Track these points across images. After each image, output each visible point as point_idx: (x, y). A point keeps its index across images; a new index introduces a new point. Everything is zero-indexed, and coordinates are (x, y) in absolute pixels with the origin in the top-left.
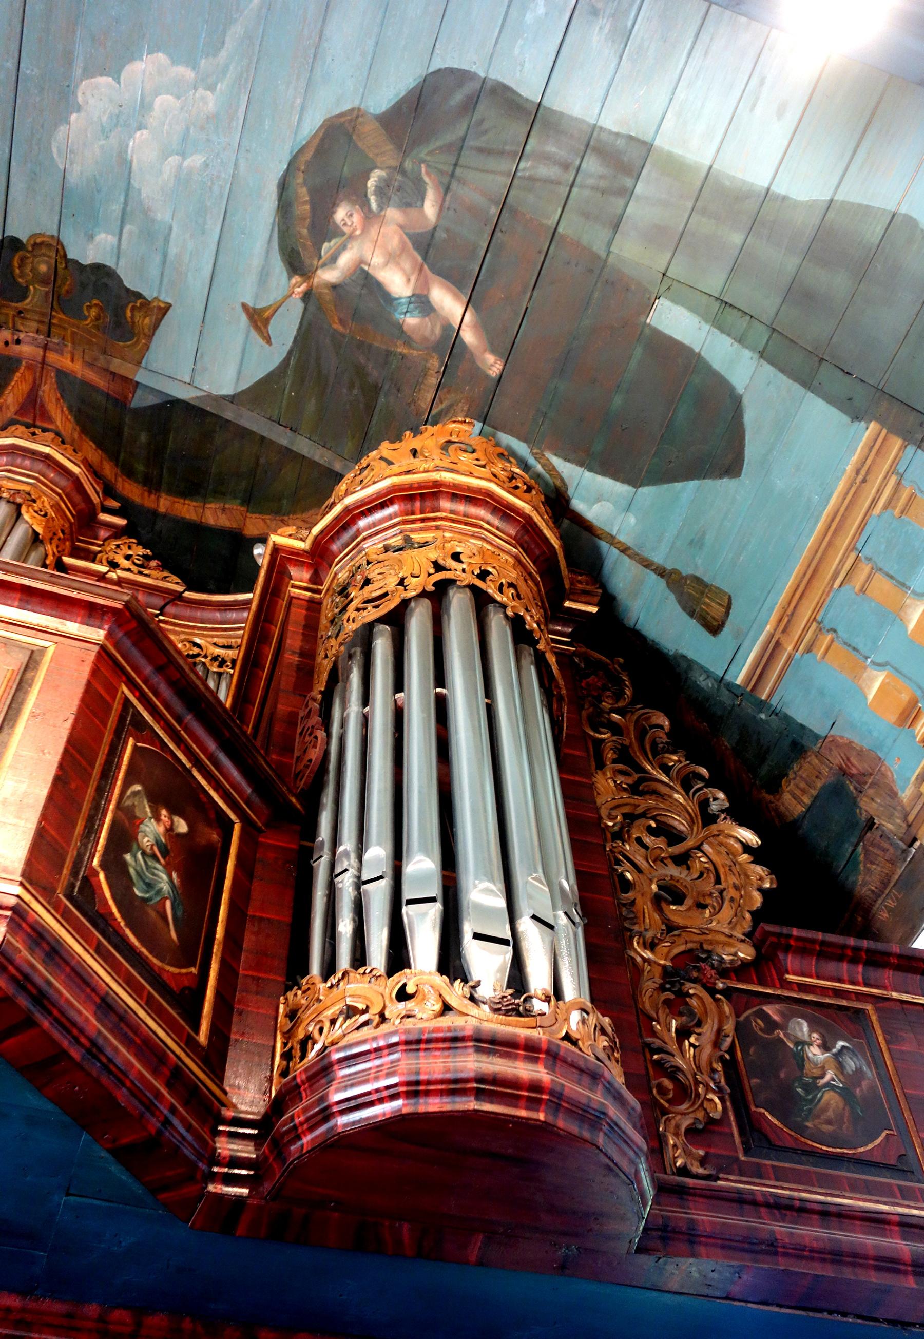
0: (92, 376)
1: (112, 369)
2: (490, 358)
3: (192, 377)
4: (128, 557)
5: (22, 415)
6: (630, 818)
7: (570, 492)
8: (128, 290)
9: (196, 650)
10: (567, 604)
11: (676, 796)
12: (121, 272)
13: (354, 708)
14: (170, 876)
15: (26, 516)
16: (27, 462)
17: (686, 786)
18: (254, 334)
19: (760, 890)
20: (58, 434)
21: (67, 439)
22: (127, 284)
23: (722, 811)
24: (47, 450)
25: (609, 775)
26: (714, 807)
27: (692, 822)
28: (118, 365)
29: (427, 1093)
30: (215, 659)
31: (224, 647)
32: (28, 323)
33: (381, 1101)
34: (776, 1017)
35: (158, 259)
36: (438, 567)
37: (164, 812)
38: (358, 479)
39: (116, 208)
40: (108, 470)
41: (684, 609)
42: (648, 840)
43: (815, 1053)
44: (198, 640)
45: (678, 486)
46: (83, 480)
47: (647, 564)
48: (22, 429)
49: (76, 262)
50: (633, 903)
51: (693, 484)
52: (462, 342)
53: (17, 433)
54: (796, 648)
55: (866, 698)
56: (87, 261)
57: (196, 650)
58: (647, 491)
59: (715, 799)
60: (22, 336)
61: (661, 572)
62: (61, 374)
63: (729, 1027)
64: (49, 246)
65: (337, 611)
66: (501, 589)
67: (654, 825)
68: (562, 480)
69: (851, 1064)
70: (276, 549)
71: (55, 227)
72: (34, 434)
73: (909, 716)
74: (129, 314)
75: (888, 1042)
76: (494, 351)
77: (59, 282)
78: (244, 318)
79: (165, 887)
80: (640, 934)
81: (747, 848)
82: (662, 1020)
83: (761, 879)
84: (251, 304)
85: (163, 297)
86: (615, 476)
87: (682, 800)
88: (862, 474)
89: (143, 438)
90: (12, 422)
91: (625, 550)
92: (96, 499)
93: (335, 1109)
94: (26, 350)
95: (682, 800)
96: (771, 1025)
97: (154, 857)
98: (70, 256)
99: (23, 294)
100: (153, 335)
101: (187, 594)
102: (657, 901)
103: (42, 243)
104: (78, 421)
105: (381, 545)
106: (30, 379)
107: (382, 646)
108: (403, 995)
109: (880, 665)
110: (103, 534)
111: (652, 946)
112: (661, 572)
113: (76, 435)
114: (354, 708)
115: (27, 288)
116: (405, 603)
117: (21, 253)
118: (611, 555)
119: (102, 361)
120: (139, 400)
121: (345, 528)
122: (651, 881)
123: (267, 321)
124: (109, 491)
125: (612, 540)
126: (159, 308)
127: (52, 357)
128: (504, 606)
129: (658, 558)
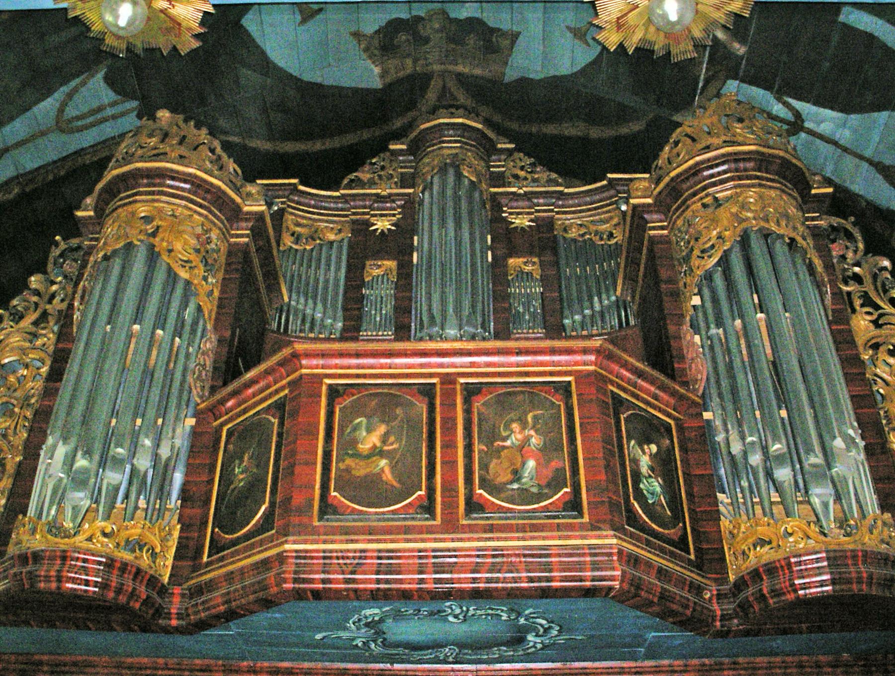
2: (736, 45)
4: (522, 168)
6: (876, 347)
14: (658, 481)
18: (578, 42)
24: (460, 120)
29: (810, 588)
37: (646, 447)
38: (675, 151)
40: (497, 118)
47: (861, 157)
58: (855, 118)
66: (778, 223)
67: (891, 347)
70: (635, 207)
78: (569, 35)
84: (573, 26)
85: (515, 28)
86: (832, 109)
97: (650, 476)
101: (566, 191)
107: (719, 281)
112: (870, 162)
120: (507, 79)
123: (585, 34)
128: (781, 237)
129: (868, 153)
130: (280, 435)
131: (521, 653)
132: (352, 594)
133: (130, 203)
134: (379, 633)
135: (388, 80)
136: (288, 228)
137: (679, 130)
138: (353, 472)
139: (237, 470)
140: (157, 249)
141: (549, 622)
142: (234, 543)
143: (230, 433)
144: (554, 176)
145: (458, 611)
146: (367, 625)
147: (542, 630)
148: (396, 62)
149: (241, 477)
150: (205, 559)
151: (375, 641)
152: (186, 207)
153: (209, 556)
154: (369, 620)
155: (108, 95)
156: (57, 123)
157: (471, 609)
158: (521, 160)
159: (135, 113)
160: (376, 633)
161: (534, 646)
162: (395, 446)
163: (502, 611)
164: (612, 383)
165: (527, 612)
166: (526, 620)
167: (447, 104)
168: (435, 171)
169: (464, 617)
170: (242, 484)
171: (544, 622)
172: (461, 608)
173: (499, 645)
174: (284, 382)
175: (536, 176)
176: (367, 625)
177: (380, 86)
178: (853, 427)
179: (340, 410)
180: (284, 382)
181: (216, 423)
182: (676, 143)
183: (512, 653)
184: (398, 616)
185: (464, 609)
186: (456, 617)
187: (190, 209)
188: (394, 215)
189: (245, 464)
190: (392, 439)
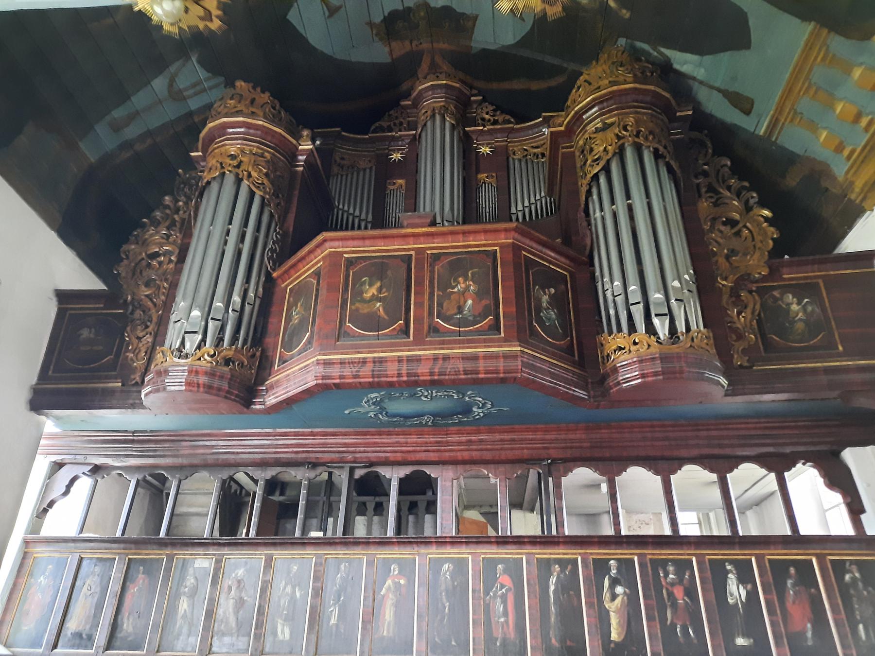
2: (624, 11)
3: (495, 40)
4: (487, 113)
6: (714, 220)
7: (672, 61)
9: (526, 153)
10: (678, 114)
11: (734, 202)
12: (454, 6)
13: (598, 214)
14: (554, 312)
15: (448, 119)
17: (738, 195)
19: (773, 239)
22: (458, 10)
23: (755, 203)
25: (704, 200)
26: (752, 201)
27: (741, 215)
29: (648, 377)
30: (534, 154)
31: (537, 147)
33: (634, 380)
34: (778, 296)
36: (619, 138)
38: (578, 93)
41: (732, 105)
42: (722, 228)
43: (795, 307)
44: (525, 148)
45: (722, 54)
47: (712, 87)
49: (435, 8)
50: (717, 261)
51: (728, 53)
52: (610, 6)
54: (786, 120)
55: (819, 140)
56: (439, 6)
57: (526, 153)
58: (708, 59)
59: (752, 197)
60: (422, 41)
61: (719, 90)
63: (758, 307)
65: (582, 163)
68: (667, 57)
69: (810, 308)
72: (438, 77)
73: (839, 149)
74: (461, 21)
75: (827, 294)
76: (626, 8)
79: (554, 316)
80: (721, 275)
81: (766, 219)
82: (731, 310)
83: (773, 233)
85: (474, 12)
86: (692, 53)
87: (736, 204)
88: (809, 47)
90: (428, 74)
91: (701, 82)
92: (468, 93)
93: (622, 382)
95: (736, 204)
96: (776, 299)
100: (474, 26)
102: (728, 257)
105: (594, 128)
107: (602, 180)
108: (635, 343)
109: (825, 128)
110: (475, 106)
111: (726, 279)
112: (719, 90)
114: (598, 214)
115: (418, 23)
116: (608, 162)
118: (696, 86)
120: (473, 52)
121: (578, 119)
122: (724, 249)
124: (471, 88)
125: (694, 79)
126: (473, 17)
127: (435, 45)
129: (717, 85)
130: (317, 290)
131: (472, 419)
132: (358, 385)
133: (223, 146)
134: (382, 409)
136: (336, 161)
137: (581, 78)
140: (240, 177)
141: (483, 399)
142: (292, 357)
144: (508, 117)
145: (426, 394)
146: (374, 404)
147: (481, 405)
149: (296, 317)
151: (381, 414)
152: (258, 147)
153: (278, 366)
154: (374, 400)
155: (202, 74)
157: (434, 392)
158: (487, 107)
159: (223, 85)
160: (380, 408)
161: (478, 415)
162: (386, 294)
163: (453, 393)
164: (525, 250)
165: (469, 393)
166: (469, 398)
167: (434, 70)
168: (428, 118)
169: (431, 397)
170: (296, 321)
171: (481, 399)
172: (428, 391)
173: (457, 414)
174: (320, 257)
175: (496, 118)
176: (374, 404)
178: (688, 273)
180: (320, 257)
181: (283, 286)
182: (579, 88)
183: (466, 419)
184: (391, 398)
185: (430, 392)
186: (426, 397)
187: (262, 149)
188: (404, 149)
190: (384, 290)
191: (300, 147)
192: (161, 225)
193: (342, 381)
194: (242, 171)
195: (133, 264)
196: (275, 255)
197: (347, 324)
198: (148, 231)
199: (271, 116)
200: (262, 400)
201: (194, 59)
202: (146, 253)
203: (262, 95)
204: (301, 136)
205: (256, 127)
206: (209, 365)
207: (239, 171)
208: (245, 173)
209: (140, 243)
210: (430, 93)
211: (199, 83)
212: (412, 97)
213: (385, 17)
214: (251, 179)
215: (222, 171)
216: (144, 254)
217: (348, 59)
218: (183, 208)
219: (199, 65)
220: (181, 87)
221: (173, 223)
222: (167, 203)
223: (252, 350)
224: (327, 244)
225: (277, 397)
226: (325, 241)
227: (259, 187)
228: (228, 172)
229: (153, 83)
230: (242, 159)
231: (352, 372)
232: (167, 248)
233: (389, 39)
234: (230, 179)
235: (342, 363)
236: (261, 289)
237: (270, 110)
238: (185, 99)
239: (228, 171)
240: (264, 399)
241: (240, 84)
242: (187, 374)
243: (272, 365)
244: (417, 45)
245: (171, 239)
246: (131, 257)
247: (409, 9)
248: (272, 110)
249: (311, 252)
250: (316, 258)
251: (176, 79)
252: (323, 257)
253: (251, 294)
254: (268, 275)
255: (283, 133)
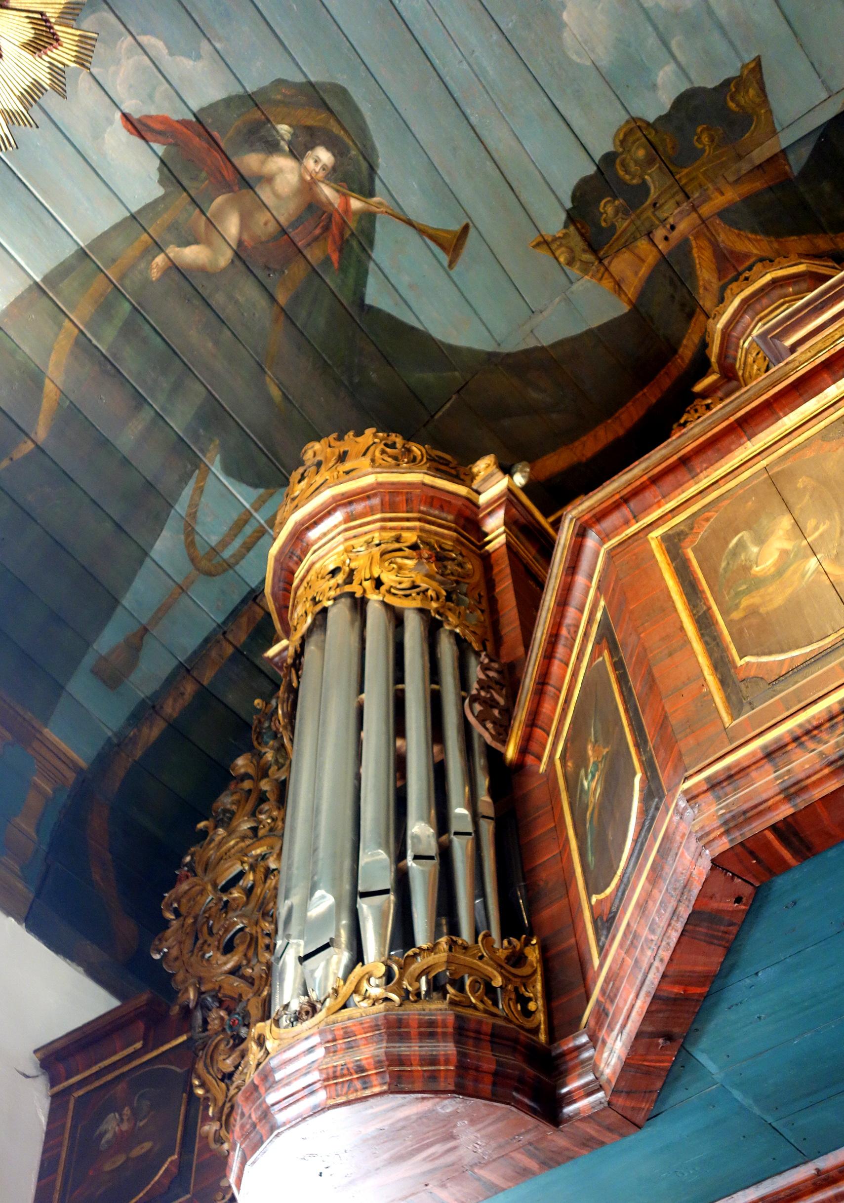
0: (747, 188)
1: (758, 162)
3: (828, 89)
5: (725, 277)
8: (715, 89)
12: (699, 83)
16: (765, 301)
20: (761, 260)
21: (770, 254)
22: (711, 85)
24: (768, 278)
28: (760, 155)
32: (666, 207)
35: (716, 37)
39: (652, 41)
46: (814, 269)
48: (734, 285)
49: (660, 119)
53: (735, 291)
56: (668, 107)
60: (671, 220)
62: (723, 214)
64: (630, 132)
71: (623, 112)
72: (747, 279)
74: (732, 105)
77: (661, 149)
89: (826, 187)
90: (723, 289)
94: (683, 226)
98: (651, 118)
99: (644, 188)
100: (766, 96)
103: (625, 136)
104: (767, 233)
106: (704, 243)
113: (776, 245)
117: (618, 161)
119: (745, 167)
120: (797, 162)
126: (752, 71)
127: (706, 210)
135: (631, 292)
138: (762, 610)
139: (586, 784)
140: (358, 595)
143: (563, 758)
148: (626, 256)
149: (594, 784)
150: (596, 962)
152: (383, 529)
156: (193, 560)
162: (822, 528)
177: (625, 308)
179: (695, 550)
181: (543, 768)
187: (391, 529)
189: (592, 760)
190: (811, 524)
191: (483, 499)
192: (237, 816)
193: (802, 802)
194: (361, 584)
195: (190, 921)
196: (496, 712)
197: (740, 663)
198: (212, 840)
199: (389, 460)
200: (591, 1077)
201: (216, 468)
202: (215, 885)
203: (359, 439)
204: (473, 477)
205: (364, 494)
206: (380, 1007)
207: (355, 588)
208: (367, 584)
209: (199, 871)
210: (747, 318)
211: (245, 518)
212: (713, 359)
213: (568, 212)
214: (383, 589)
215: (319, 608)
216: (209, 887)
217: (531, 343)
218: (276, 761)
219: (232, 480)
220: (214, 540)
221: (262, 798)
222: (242, 770)
223: (505, 942)
224: (591, 541)
225: (624, 1026)
226: (581, 534)
227: (410, 595)
228: (331, 603)
229: (154, 554)
230: (353, 565)
231: (821, 754)
232: (259, 851)
233: (600, 261)
234: (339, 615)
235: (771, 754)
236: (484, 798)
237: (383, 452)
238: (229, 566)
239: (329, 599)
240: (595, 1069)
241: (315, 450)
242: (320, 1052)
243: (583, 963)
244: (666, 238)
245: (261, 833)
246: (183, 910)
247: (609, 158)
248: (388, 450)
249: (563, 602)
250: (581, 610)
251: (198, 528)
252: (598, 588)
253: (459, 810)
254: (494, 757)
255: (429, 480)
